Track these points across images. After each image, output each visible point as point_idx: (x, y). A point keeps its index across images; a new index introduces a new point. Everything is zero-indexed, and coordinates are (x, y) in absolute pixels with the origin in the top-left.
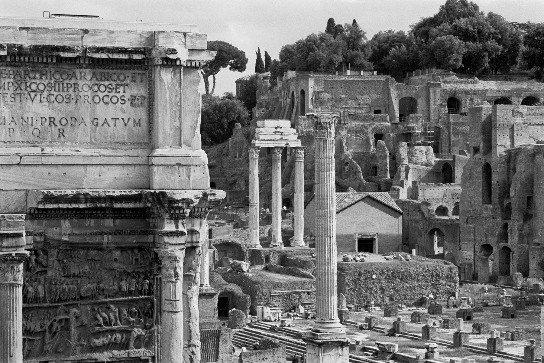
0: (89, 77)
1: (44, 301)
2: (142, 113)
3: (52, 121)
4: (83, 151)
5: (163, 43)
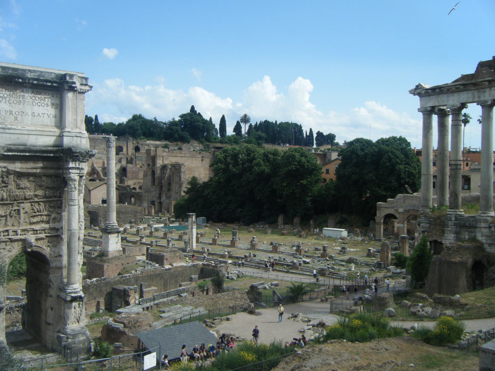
1: (7, 200)
4: (28, 128)
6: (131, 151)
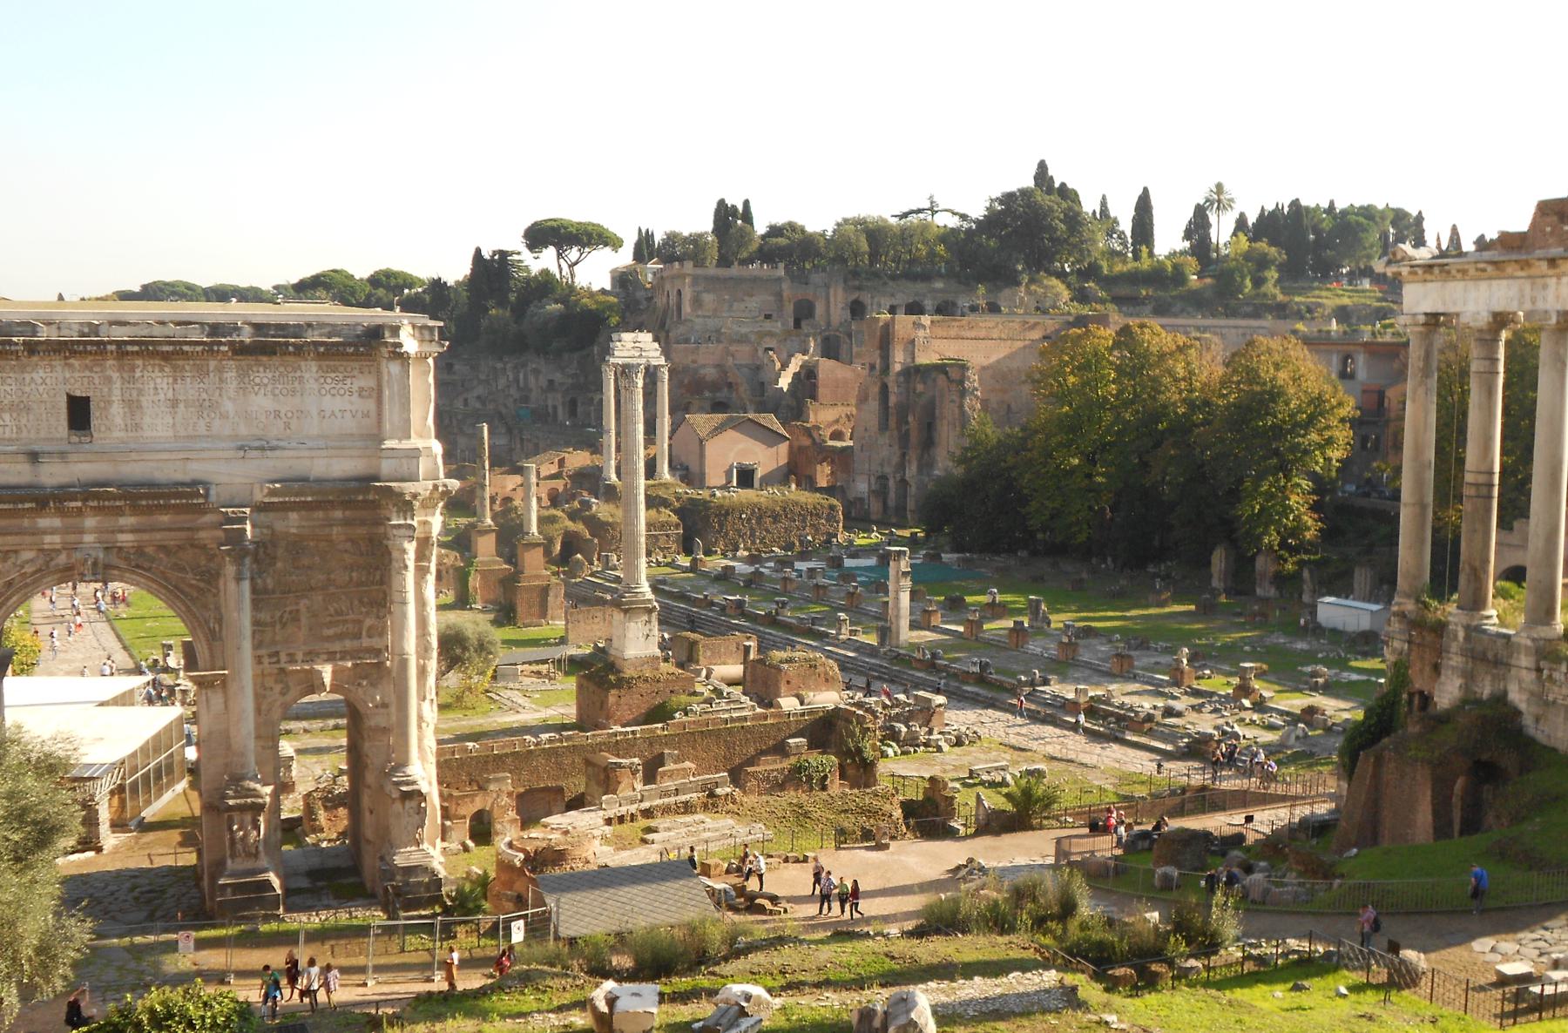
0: (314, 369)
2: (371, 405)
3: (277, 414)
4: (310, 444)
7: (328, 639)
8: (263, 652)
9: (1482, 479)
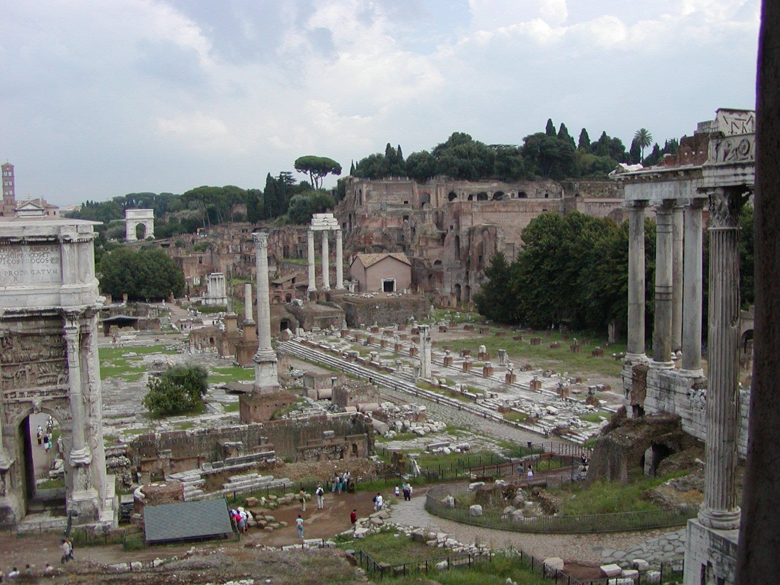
0: (28, 250)
2: (57, 267)
4: (26, 288)
5: (63, 233)
6: (443, 200)
7: (41, 385)
8: (8, 391)
9: (662, 290)
